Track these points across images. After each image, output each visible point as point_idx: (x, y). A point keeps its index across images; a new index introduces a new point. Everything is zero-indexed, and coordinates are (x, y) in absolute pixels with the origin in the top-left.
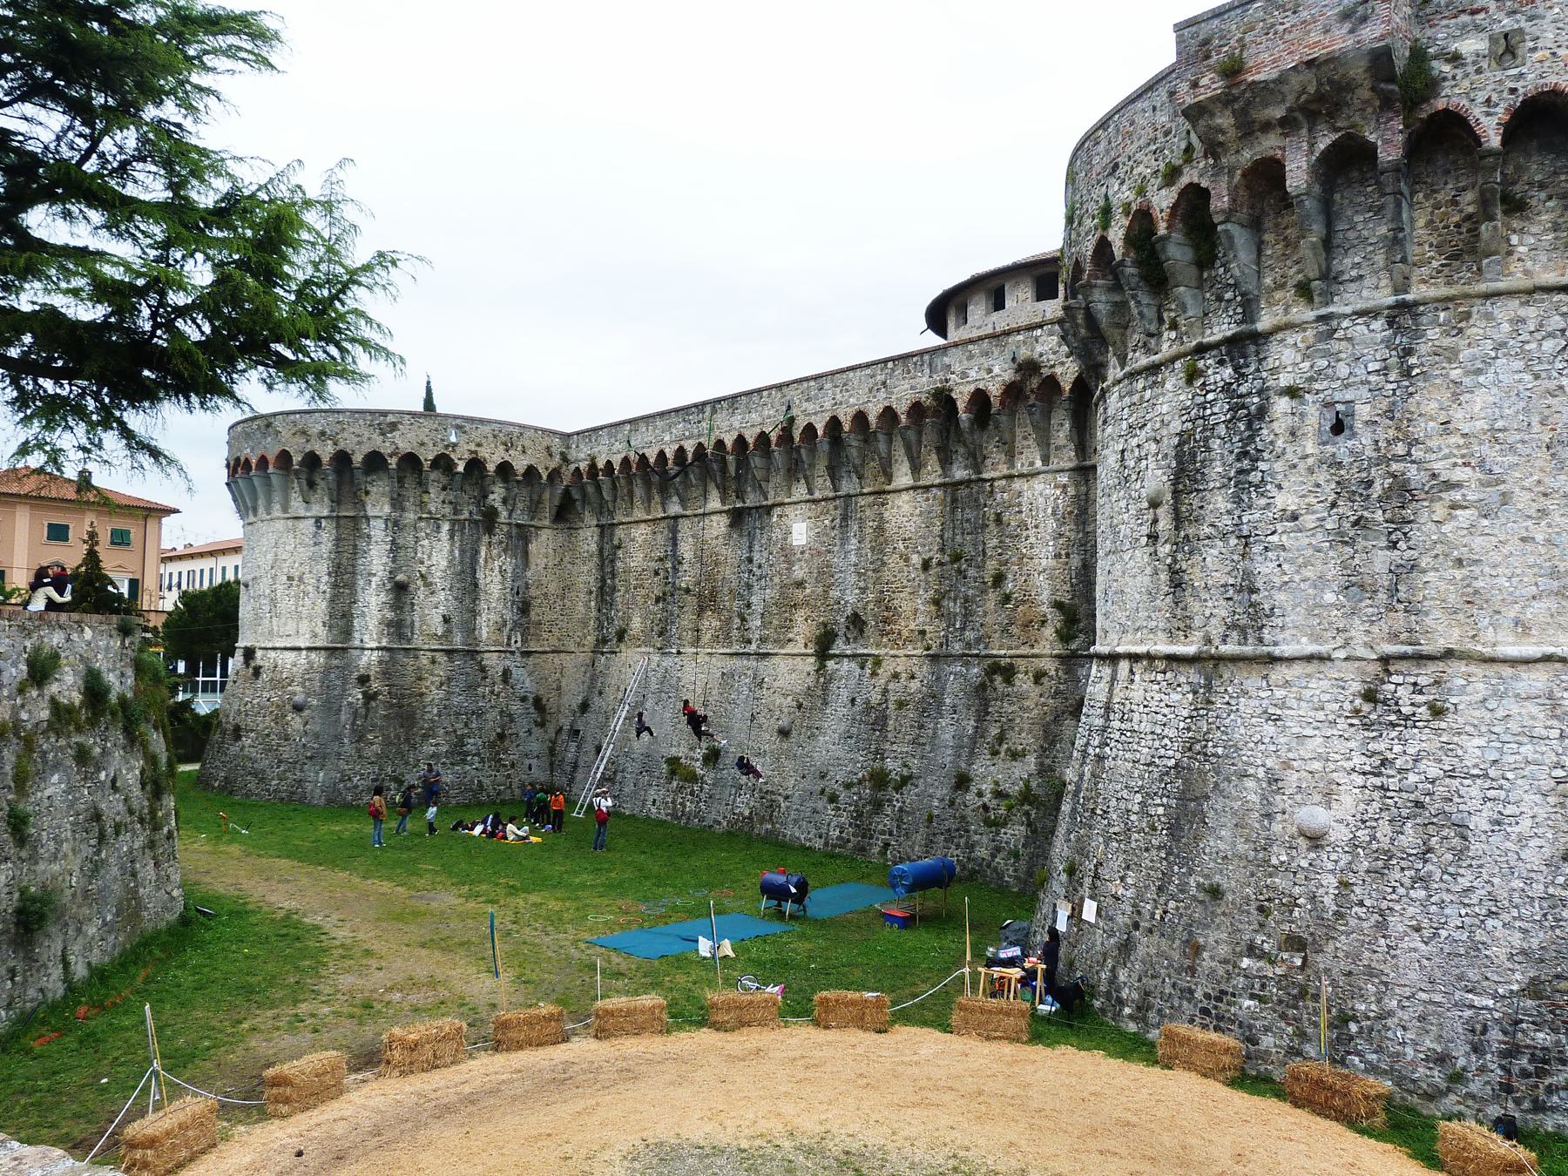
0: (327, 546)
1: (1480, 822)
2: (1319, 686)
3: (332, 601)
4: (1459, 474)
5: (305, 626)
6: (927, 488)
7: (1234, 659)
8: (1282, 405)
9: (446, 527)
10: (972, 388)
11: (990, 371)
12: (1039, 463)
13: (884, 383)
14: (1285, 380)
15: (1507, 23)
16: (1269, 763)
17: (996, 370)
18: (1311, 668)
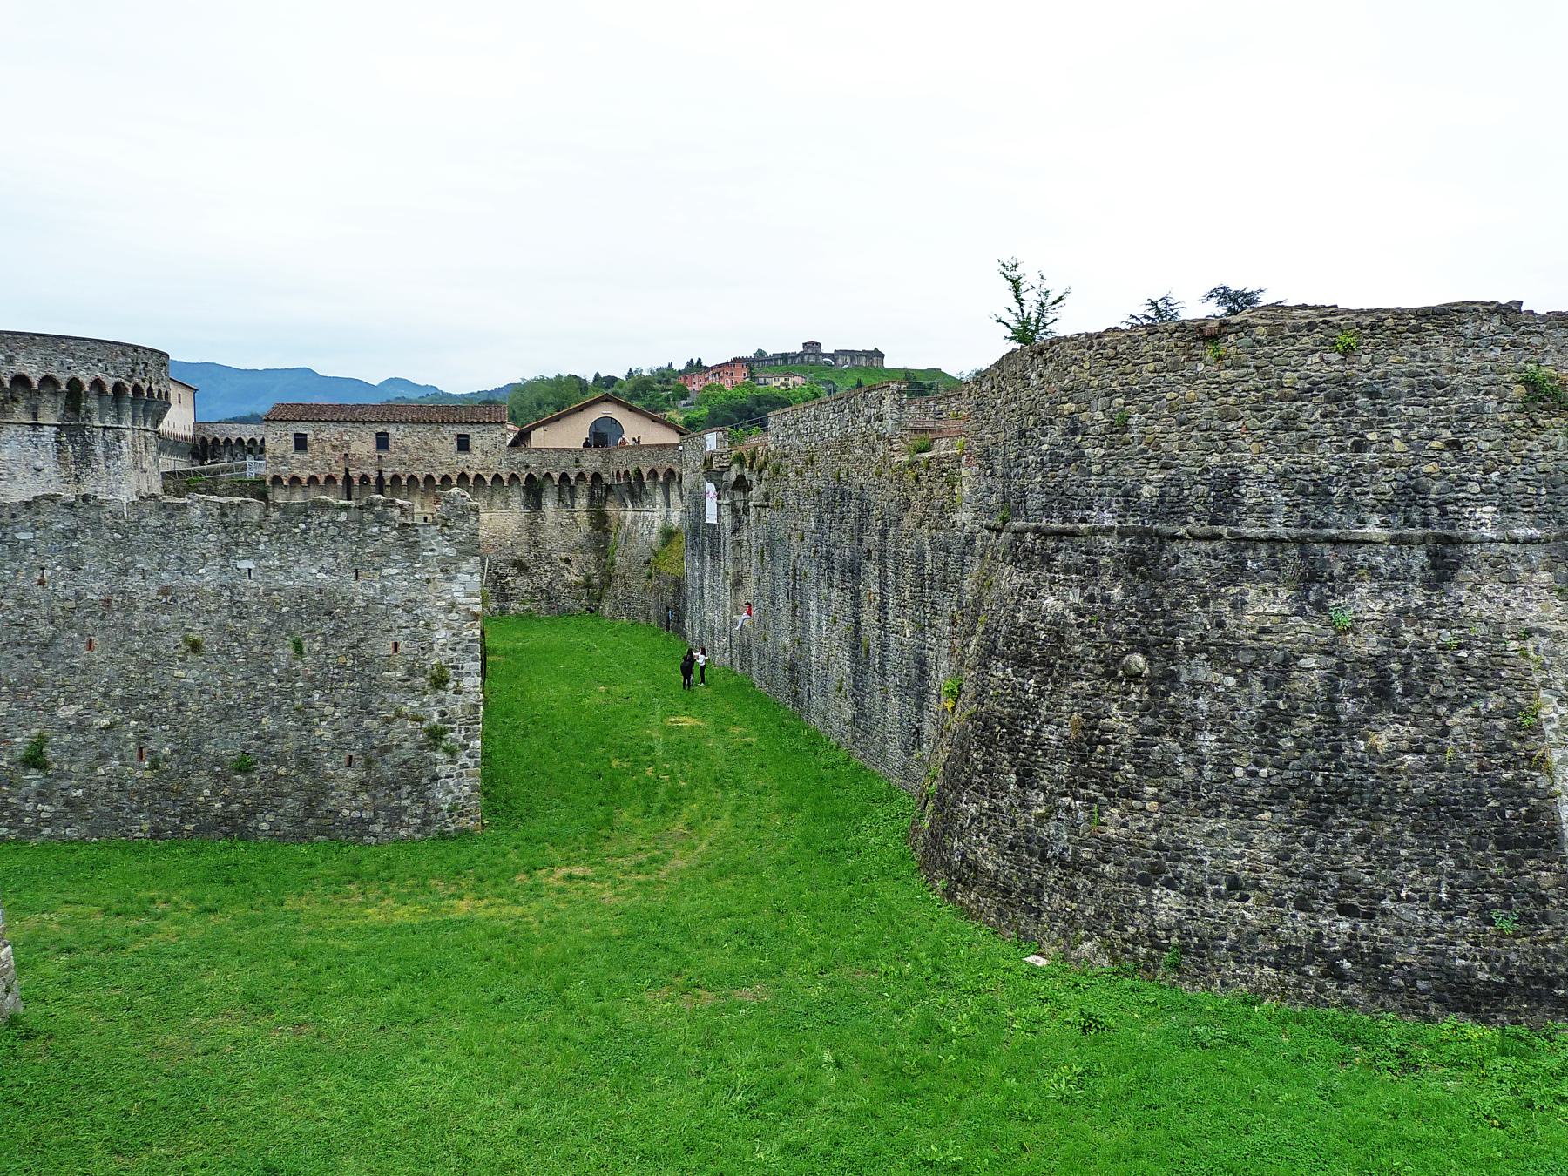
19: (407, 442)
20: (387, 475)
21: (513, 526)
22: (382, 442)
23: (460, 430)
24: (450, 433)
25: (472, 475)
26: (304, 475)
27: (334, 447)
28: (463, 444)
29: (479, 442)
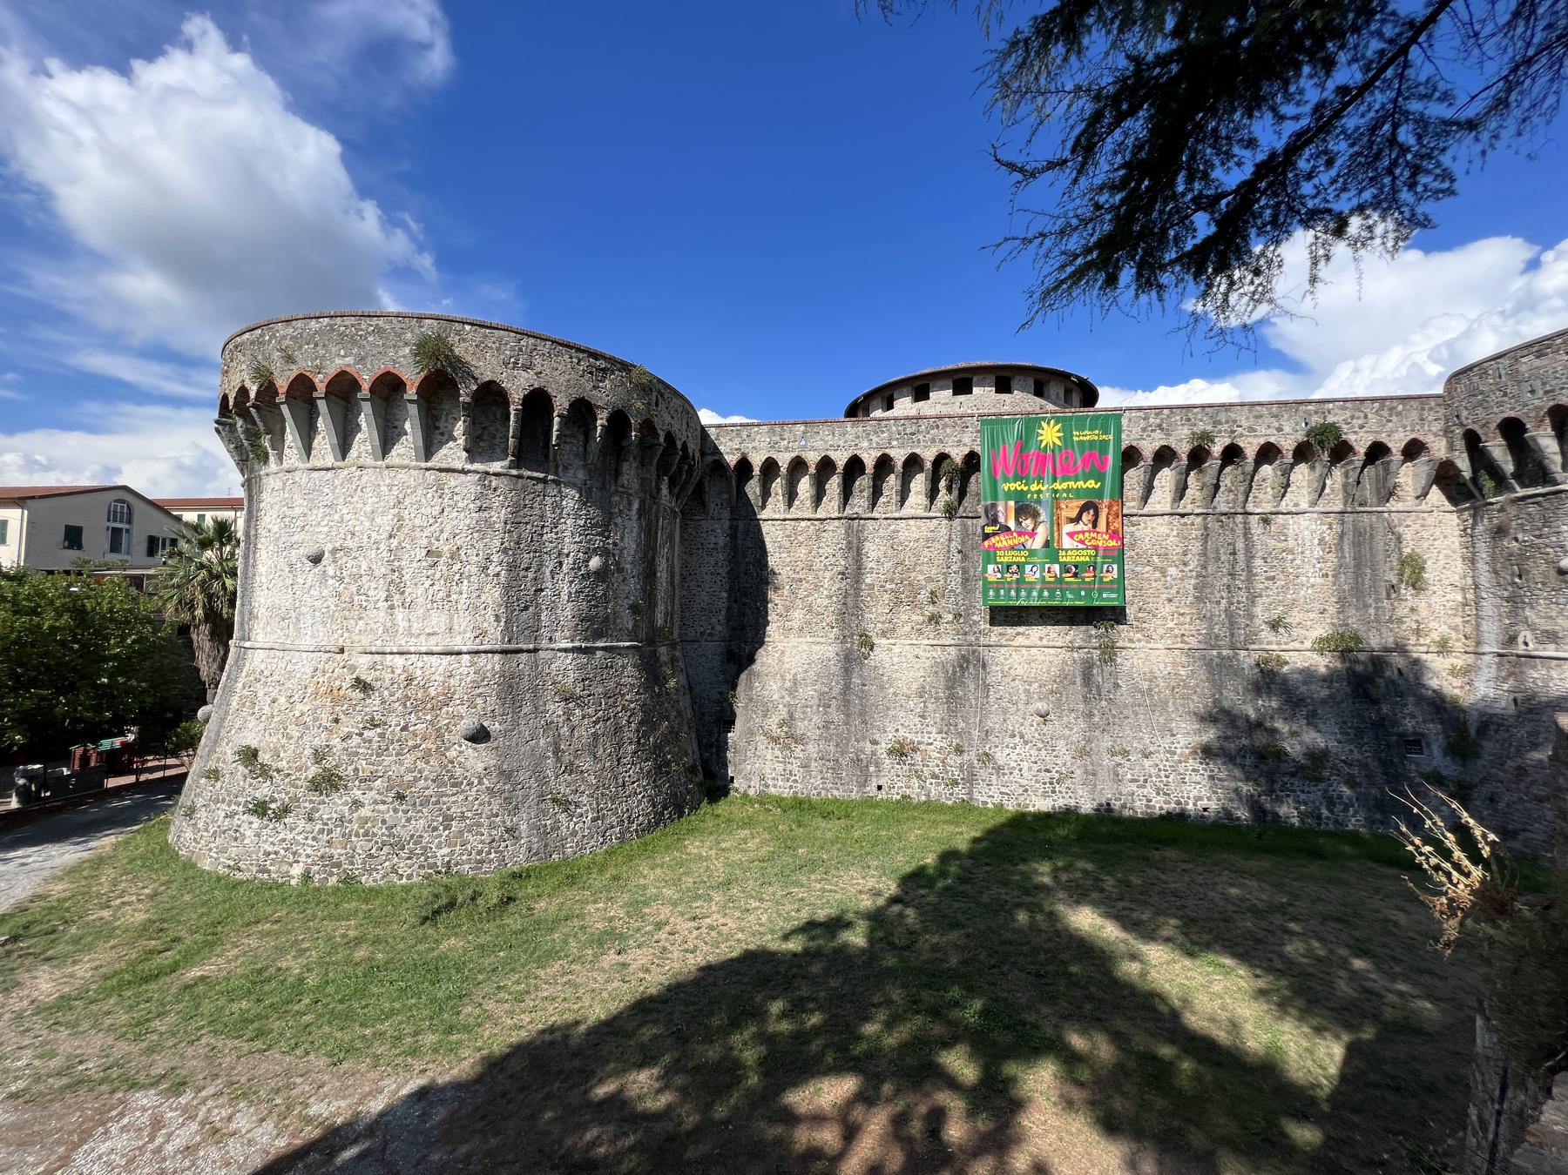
0: (499, 515)
3: (508, 588)
5: (463, 622)
6: (1183, 516)
9: (636, 506)
10: (1262, 441)
11: (1280, 429)
12: (1304, 506)
13: (1160, 426)
17: (1287, 429)
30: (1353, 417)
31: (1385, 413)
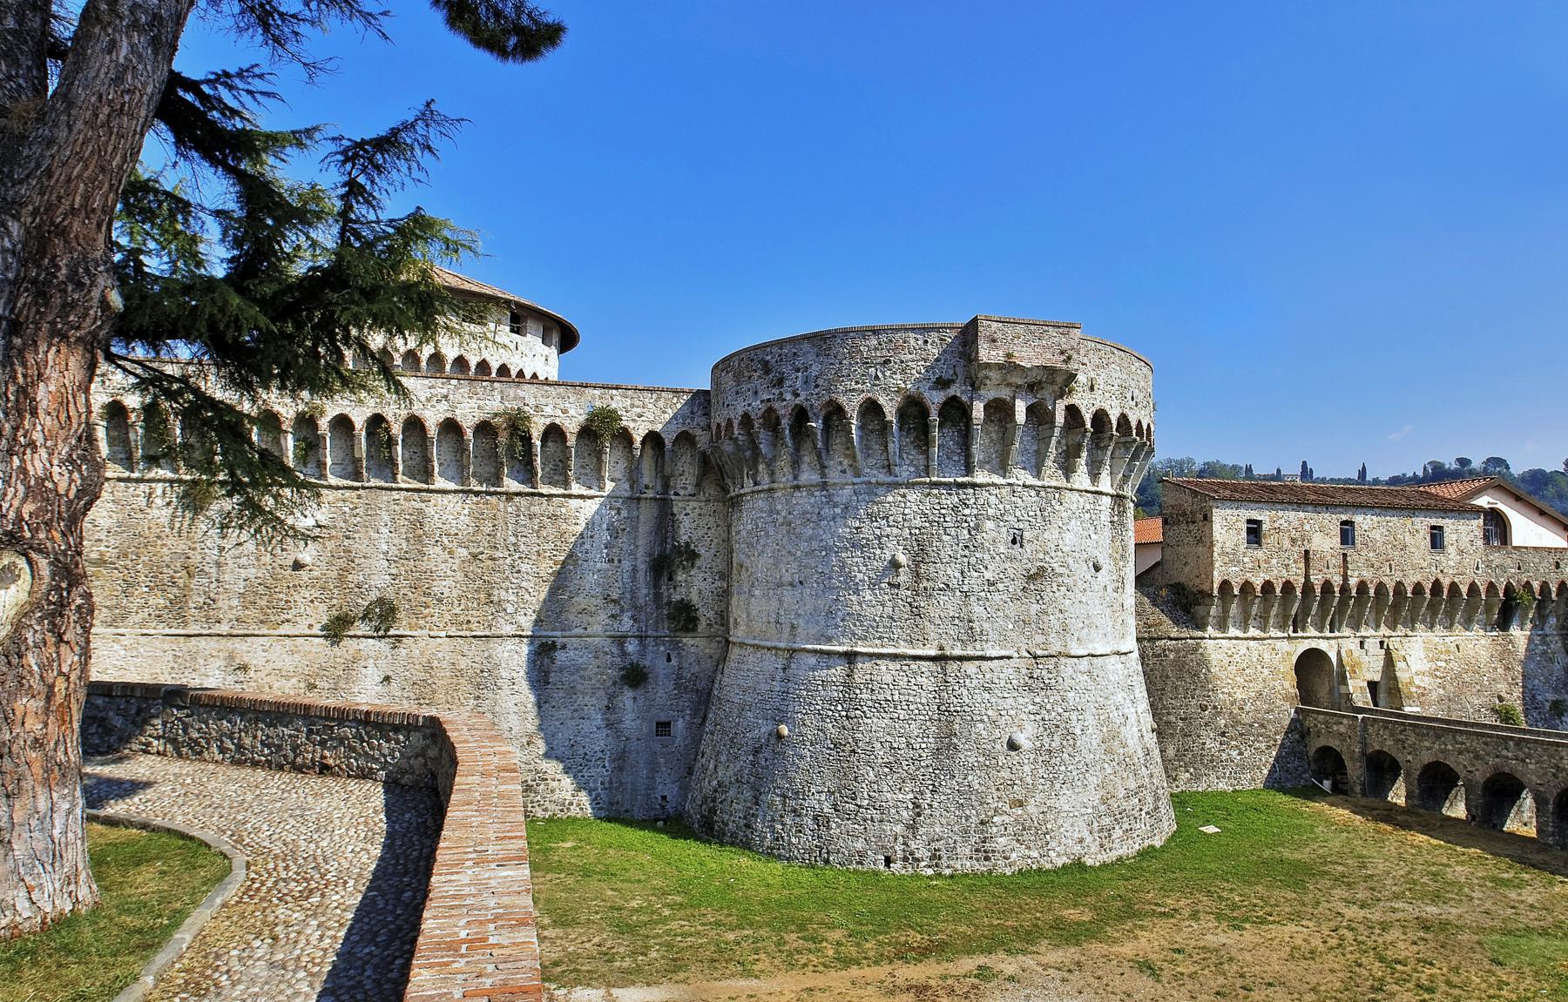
1: (1078, 731)
2: (1007, 671)
4: (1061, 570)
7: (961, 659)
8: (989, 525)
11: (564, 411)
14: (991, 512)
15: (1092, 374)
16: (990, 713)
17: (572, 412)
18: (1002, 662)
19: (1376, 534)
20: (1353, 582)
21: (1484, 656)
22: (1347, 534)
23: (1434, 522)
24: (1423, 523)
25: (1446, 582)
26: (1258, 582)
27: (1293, 541)
28: (1437, 539)
29: (1454, 537)
30: (633, 406)
31: (661, 404)
